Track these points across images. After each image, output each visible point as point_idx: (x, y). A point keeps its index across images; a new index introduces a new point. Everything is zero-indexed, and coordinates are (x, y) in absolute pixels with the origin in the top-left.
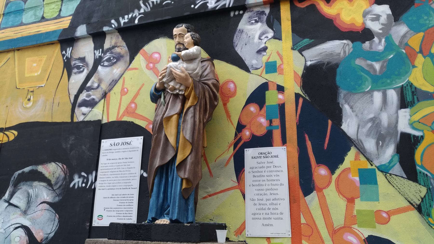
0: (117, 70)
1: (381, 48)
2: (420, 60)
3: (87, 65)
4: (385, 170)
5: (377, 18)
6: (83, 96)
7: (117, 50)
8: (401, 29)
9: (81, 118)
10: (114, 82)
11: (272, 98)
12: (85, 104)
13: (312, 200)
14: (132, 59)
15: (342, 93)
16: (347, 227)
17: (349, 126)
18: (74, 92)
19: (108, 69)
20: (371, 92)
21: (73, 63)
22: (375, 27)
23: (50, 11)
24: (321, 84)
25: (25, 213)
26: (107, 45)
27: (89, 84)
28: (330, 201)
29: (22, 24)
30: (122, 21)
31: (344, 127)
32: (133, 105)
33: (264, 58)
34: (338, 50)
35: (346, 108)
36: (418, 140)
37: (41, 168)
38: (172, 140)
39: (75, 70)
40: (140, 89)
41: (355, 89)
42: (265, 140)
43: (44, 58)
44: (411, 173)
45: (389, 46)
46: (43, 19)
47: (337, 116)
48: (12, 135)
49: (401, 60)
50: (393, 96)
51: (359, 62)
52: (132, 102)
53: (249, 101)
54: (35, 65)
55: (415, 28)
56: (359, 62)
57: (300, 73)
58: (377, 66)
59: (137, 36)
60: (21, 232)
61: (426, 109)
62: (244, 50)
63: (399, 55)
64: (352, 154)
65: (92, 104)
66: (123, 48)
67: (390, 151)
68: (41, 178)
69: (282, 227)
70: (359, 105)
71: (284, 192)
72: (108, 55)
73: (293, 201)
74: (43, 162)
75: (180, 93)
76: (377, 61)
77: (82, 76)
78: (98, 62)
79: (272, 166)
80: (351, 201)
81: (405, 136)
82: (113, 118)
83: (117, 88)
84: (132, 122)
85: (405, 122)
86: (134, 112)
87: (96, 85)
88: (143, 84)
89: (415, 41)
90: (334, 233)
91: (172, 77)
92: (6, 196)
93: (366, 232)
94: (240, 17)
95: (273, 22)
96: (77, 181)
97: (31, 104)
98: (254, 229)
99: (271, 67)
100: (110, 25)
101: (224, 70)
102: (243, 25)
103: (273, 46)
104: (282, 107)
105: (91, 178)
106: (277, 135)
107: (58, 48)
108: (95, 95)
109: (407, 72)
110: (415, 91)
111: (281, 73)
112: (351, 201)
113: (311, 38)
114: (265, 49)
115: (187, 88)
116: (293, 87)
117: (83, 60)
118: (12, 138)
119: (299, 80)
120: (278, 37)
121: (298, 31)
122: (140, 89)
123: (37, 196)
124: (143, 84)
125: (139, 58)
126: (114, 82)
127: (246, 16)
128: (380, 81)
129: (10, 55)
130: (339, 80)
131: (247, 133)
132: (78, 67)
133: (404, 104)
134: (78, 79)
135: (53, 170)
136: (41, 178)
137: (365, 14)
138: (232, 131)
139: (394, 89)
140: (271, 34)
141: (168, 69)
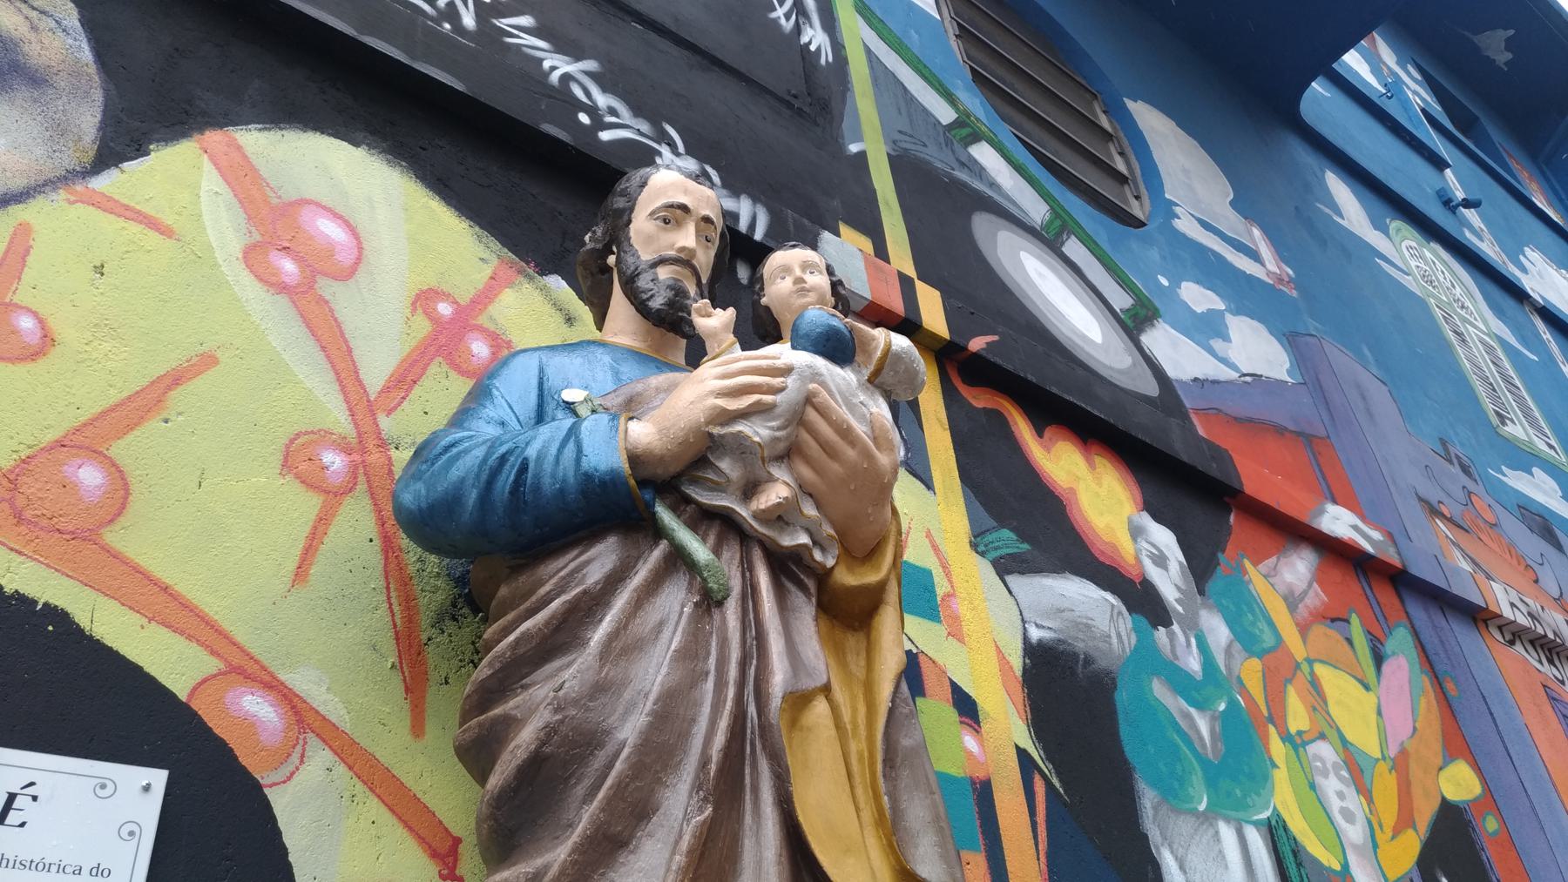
2: (1278, 748)
15: (1148, 799)
20: (1208, 818)
22: (1170, 582)
32: (90, 476)
34: (1102, 623)
35: (1168, 861)
40: (175, 379)
52: (89, 439)
56: (1159, 690)
57: (1017, 661)
63: (1232, 703)
75: (818, 555)
76: (1200, 707)
84: (58, 616)
86: (88, 536)
88: (207, 361)
104: (983, 792)
111: (956, 634)
113: (1023, 536)
119: (1019, 695)
122: (175, 379)
124: (207, 361)
139: (1256, 824)
141: (791, 381)
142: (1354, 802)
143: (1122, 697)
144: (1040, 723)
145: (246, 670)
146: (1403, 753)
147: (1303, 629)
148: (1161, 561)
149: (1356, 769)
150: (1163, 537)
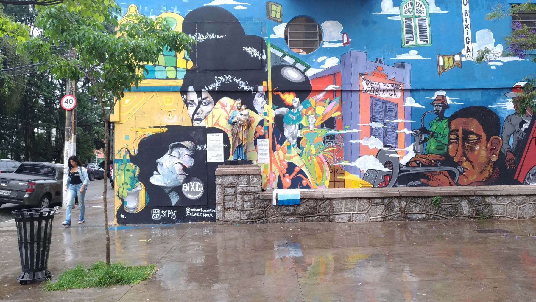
0: (209, 107)
1: (296, 112)
3: (195, 104)
4: (293, 146)
5: (296, 102)
6: (196, 116)
7: (208, 99)
8: (301, 107)
9: (197, 125)
10: (209, 113)
11: (266, 124)
12: (197, 120)
13: (275, 153)
14: (215, 104)
15: (285, 124)
16: (283, 160)
17: (286, 134)
18: (191, 114)
19: (206, 107)
21: (188, 102)
22: (295, 105)
23: (171, 75)
24: (279, 121)
25: (179, 158)
26: (203, 96)
27: (197, 112)
28: (280, 153)
29: (156, 78)
30: (210, 88)
31: (285, 134)
33: (263, 111)
35: (285, 129)
36: (301, 138)
37: (182, 143)
38: (241, 138)
39: (190, 105)
41: (288, 123)
42: (263, 137)
43: (173, 97)
44: (299, 147)
45: (298, 111)
46: (168, 78)
47: (283, 132)
48: (165, 130)
49: (299, 118)
50: (297, 126)
51: (290, 115)
52: (217, 121)
53: (259, 124)
54: (169, 100)
55: (305, 107)
56: (290, 115)
58: (294, 117)
59: (217, 95)
60: (179, 165)
61: (304, 131)
62: (257, 107)
64: (286, 141)
65: (201, 120)
66: (210, 99)
67: (295, 141)
68: (183, 146)
69: (268, 160)
70: (289, 128)
71: (268, 151)
72: (204, 101)
73: (271, 153)
74: (182, 141)
77: (194, 108)
78: (200, 103)
79: (265, 144)
80: (285, 153)
81: (299, 137)
82: (210, 126)
83: (210, 115)
85: (299, 134)
87: (201, 113)
89: (304, 111)
90: (280, 161)
91: (240, 120)
92: (169, 152)
93: (288, 161)
94: (255, 94)
95: (266, 97)
96: (199, 148)
97: (171, 117)
98: (260, 161)
99: (265, 114)
100: (205, 89)
101: (252, 113)
102: (256, 97)
103: (266, 106)
104: (268, 127)
105: (205, 147)
106: (267, 135)
107: (179, 94)
108: (202, 117)
109: (301, 120)
110: (302, 126)
112: (285, 153)
114: (263, 107)
115: (244, 123)
116: (272, 121)
117: (193, 101)
118: (165, 131)
120: (267, 104)
121: (274, 102)
123: (183, 153)
125: (218, 103)
126: (209, 113)
127: (257, 94)
128: (295, 122)
129: (154, 93)
130: (284, 120)
131: (258, 134)
132: (191, 104)
133: (299, 129)
134: (192, 109)
135: (187, 143)
136: (183, 146)
137: (293, 100)
138: (254, 133)
140: (265, 102)
142: (314, 120)
143: (285, 117)
144: (275, 121)
145: (225, 129)
146: (327, 113)
147: (316, 104)
148: (296, 102)
149: (316, 117)
150: (298, 100)
